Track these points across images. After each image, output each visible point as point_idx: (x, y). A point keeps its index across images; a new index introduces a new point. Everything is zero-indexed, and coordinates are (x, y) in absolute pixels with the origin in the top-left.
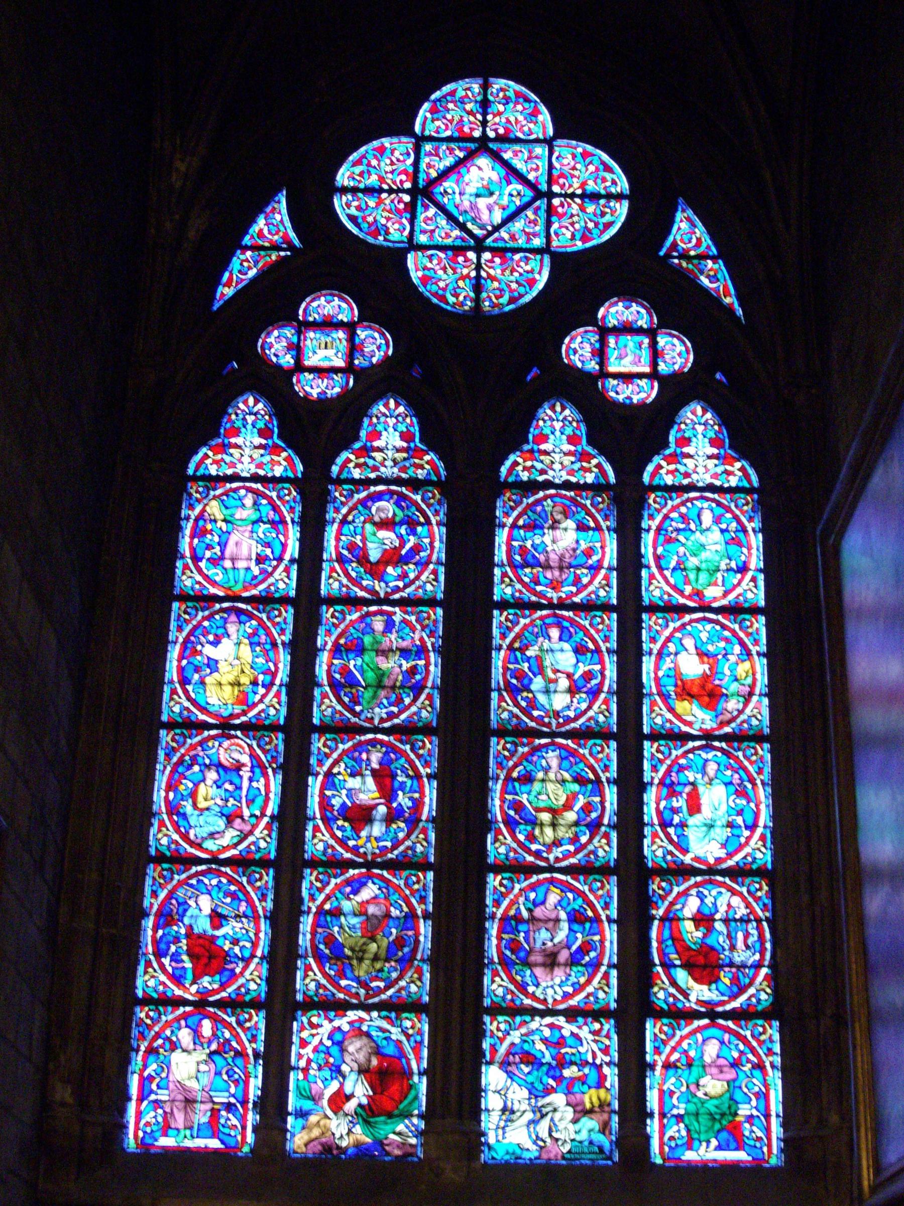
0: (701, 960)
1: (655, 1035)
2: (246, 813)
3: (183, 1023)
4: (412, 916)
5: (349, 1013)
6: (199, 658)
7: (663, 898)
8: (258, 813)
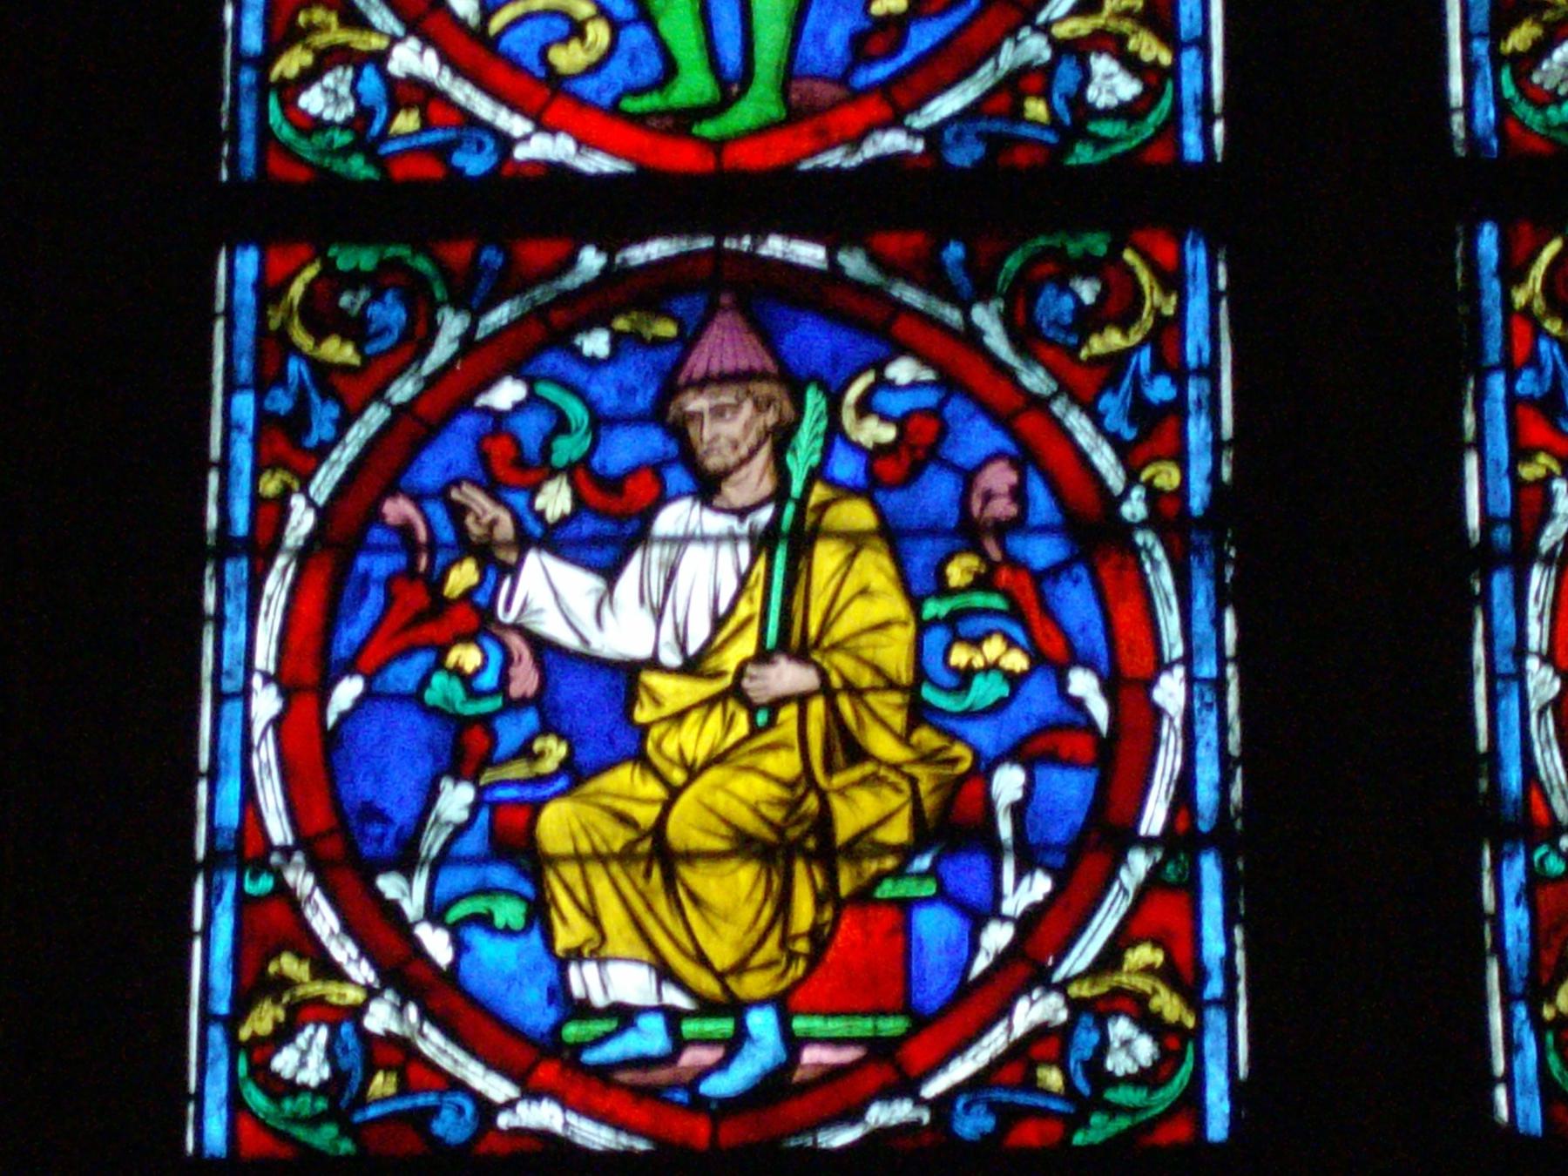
6: (467, 656)
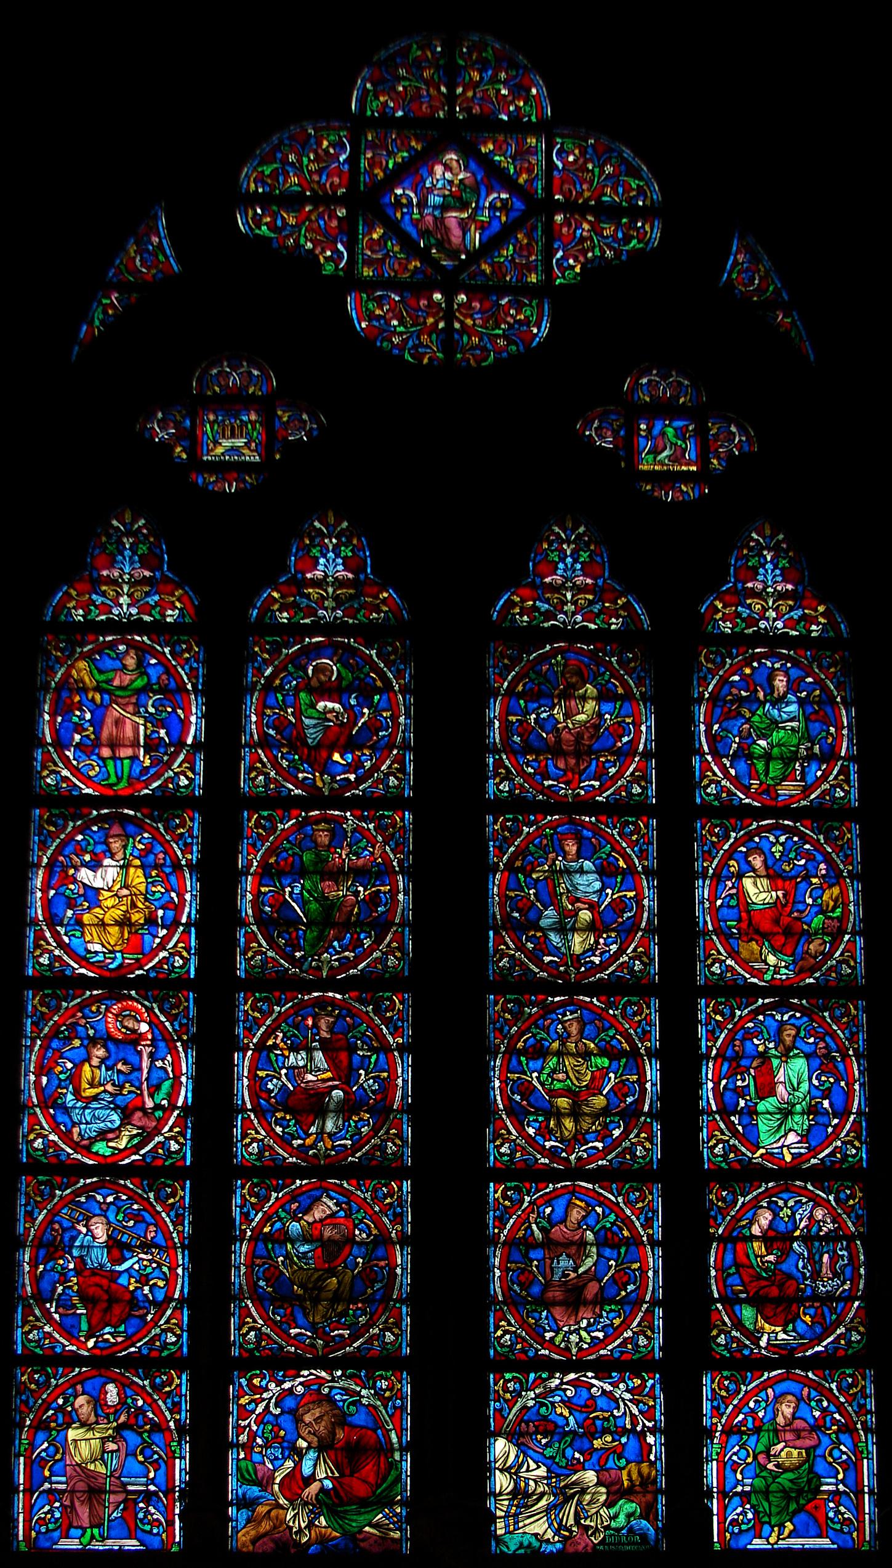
0: (774, 1292)
1: (713, 1390)
2: (149, 1104)
3: (79, 1387)
4: (382, 1240)
5: (306, 1373)
6: (72, 887)
7: (724, 1212)
8: (165, 1102)
